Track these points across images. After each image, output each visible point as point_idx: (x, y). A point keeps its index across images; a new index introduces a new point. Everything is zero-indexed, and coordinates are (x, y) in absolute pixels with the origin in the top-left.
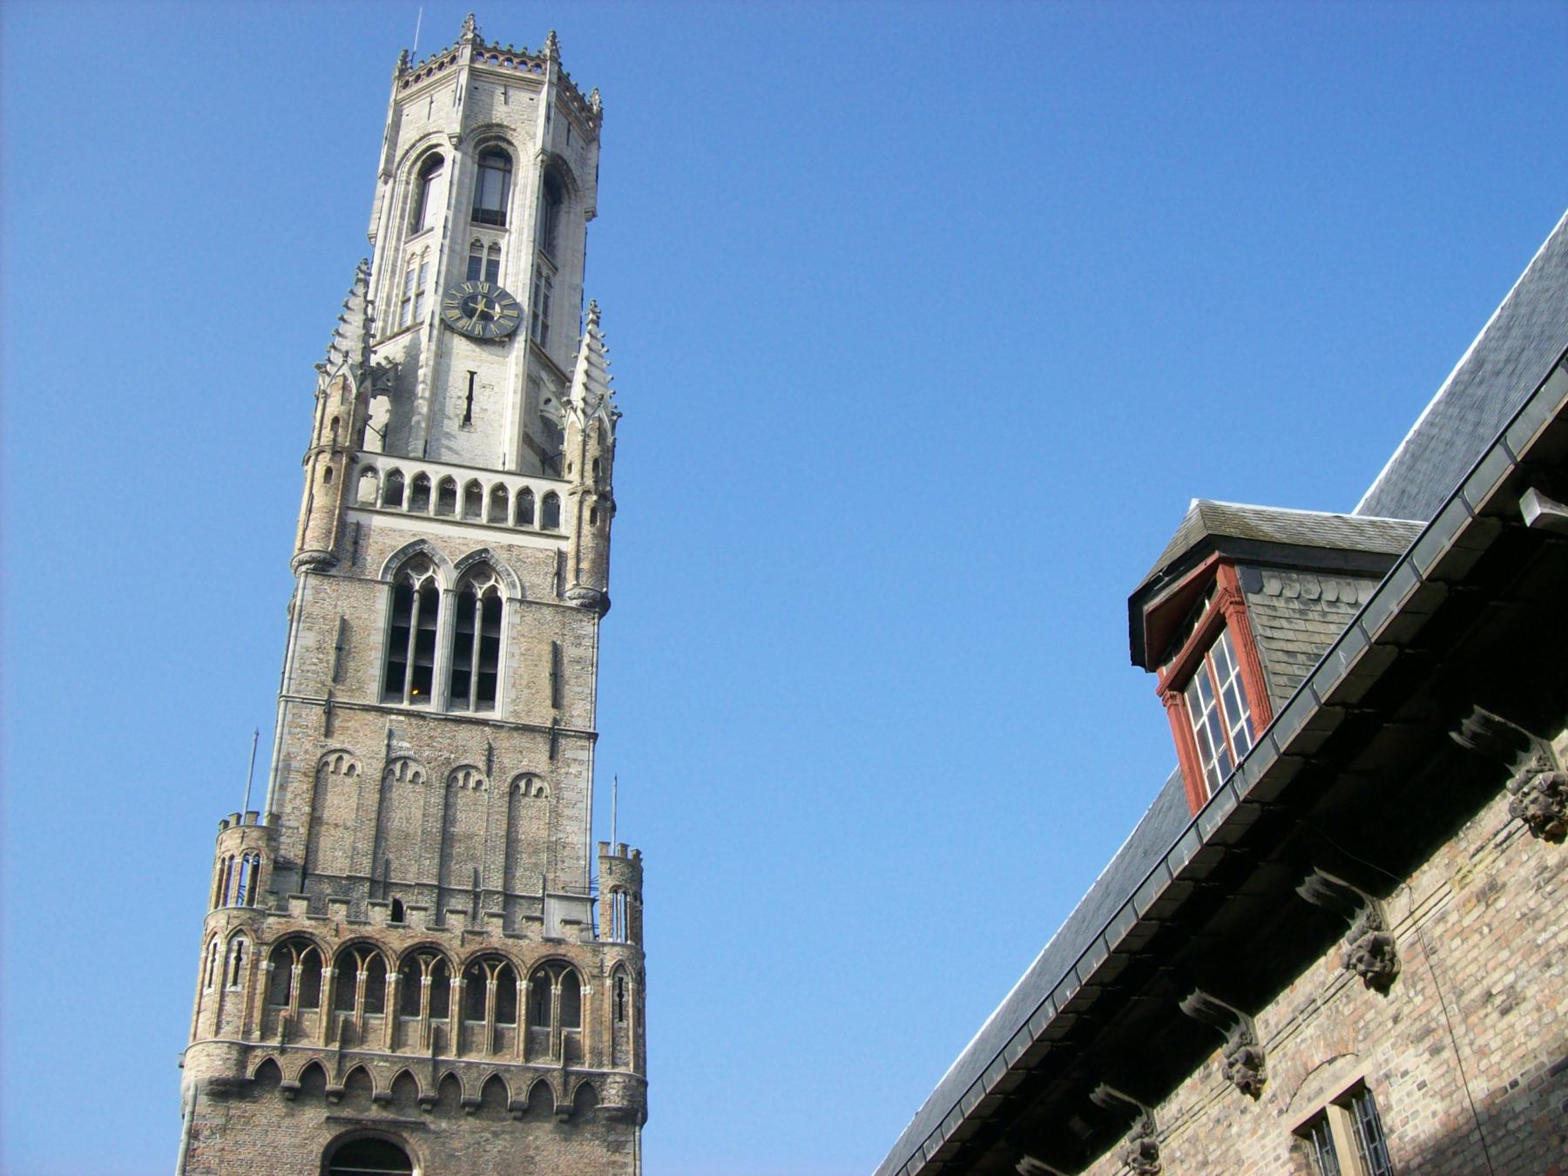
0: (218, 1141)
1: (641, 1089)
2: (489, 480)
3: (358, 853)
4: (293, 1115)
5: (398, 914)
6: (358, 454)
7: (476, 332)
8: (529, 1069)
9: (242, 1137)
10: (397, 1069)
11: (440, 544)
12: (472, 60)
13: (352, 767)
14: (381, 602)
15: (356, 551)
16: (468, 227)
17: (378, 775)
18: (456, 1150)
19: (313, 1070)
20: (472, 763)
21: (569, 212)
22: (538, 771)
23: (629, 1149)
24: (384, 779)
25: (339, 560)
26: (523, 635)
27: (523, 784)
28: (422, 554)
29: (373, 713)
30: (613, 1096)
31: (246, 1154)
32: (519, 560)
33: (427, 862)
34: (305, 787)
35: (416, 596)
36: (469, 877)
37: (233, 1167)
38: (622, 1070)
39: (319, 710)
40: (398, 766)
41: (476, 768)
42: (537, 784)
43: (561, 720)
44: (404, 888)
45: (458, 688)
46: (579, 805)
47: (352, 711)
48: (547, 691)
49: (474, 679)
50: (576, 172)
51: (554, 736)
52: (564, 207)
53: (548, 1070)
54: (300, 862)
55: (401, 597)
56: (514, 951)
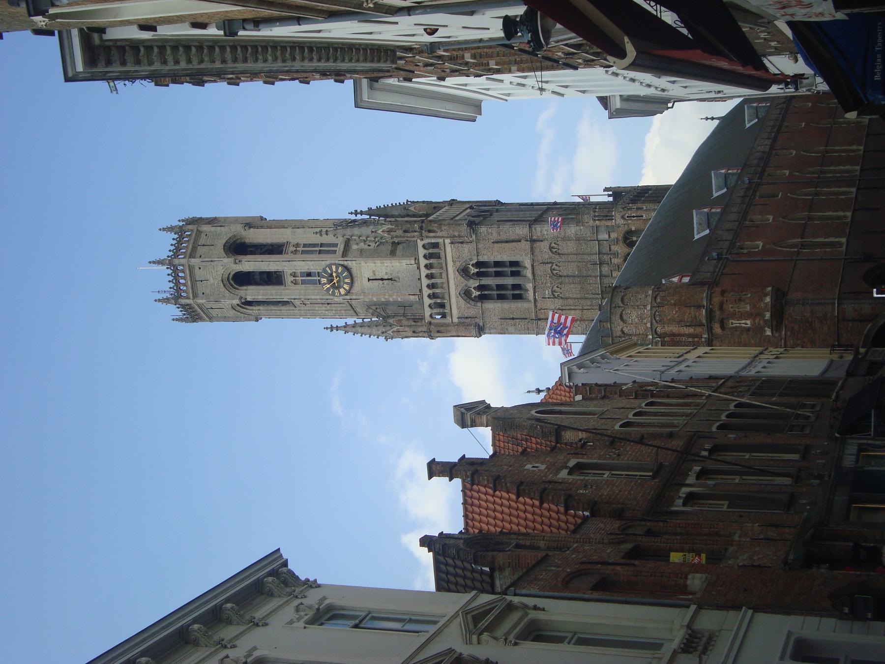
2: (424, 272)
6: (426, 321)
7: (349, 281)
11: (459, 289)
15: (470, 317)
16: (287, 287)
17: (561, 301)
20: (549, 269)
26: (492, 254)
39: (539, 322)
40: (556, 294)
41: (551, 267)
42: (553, 245)
48: (514, 243)
52: (247, 241)
55: (483, 298)
56: (623, 255)
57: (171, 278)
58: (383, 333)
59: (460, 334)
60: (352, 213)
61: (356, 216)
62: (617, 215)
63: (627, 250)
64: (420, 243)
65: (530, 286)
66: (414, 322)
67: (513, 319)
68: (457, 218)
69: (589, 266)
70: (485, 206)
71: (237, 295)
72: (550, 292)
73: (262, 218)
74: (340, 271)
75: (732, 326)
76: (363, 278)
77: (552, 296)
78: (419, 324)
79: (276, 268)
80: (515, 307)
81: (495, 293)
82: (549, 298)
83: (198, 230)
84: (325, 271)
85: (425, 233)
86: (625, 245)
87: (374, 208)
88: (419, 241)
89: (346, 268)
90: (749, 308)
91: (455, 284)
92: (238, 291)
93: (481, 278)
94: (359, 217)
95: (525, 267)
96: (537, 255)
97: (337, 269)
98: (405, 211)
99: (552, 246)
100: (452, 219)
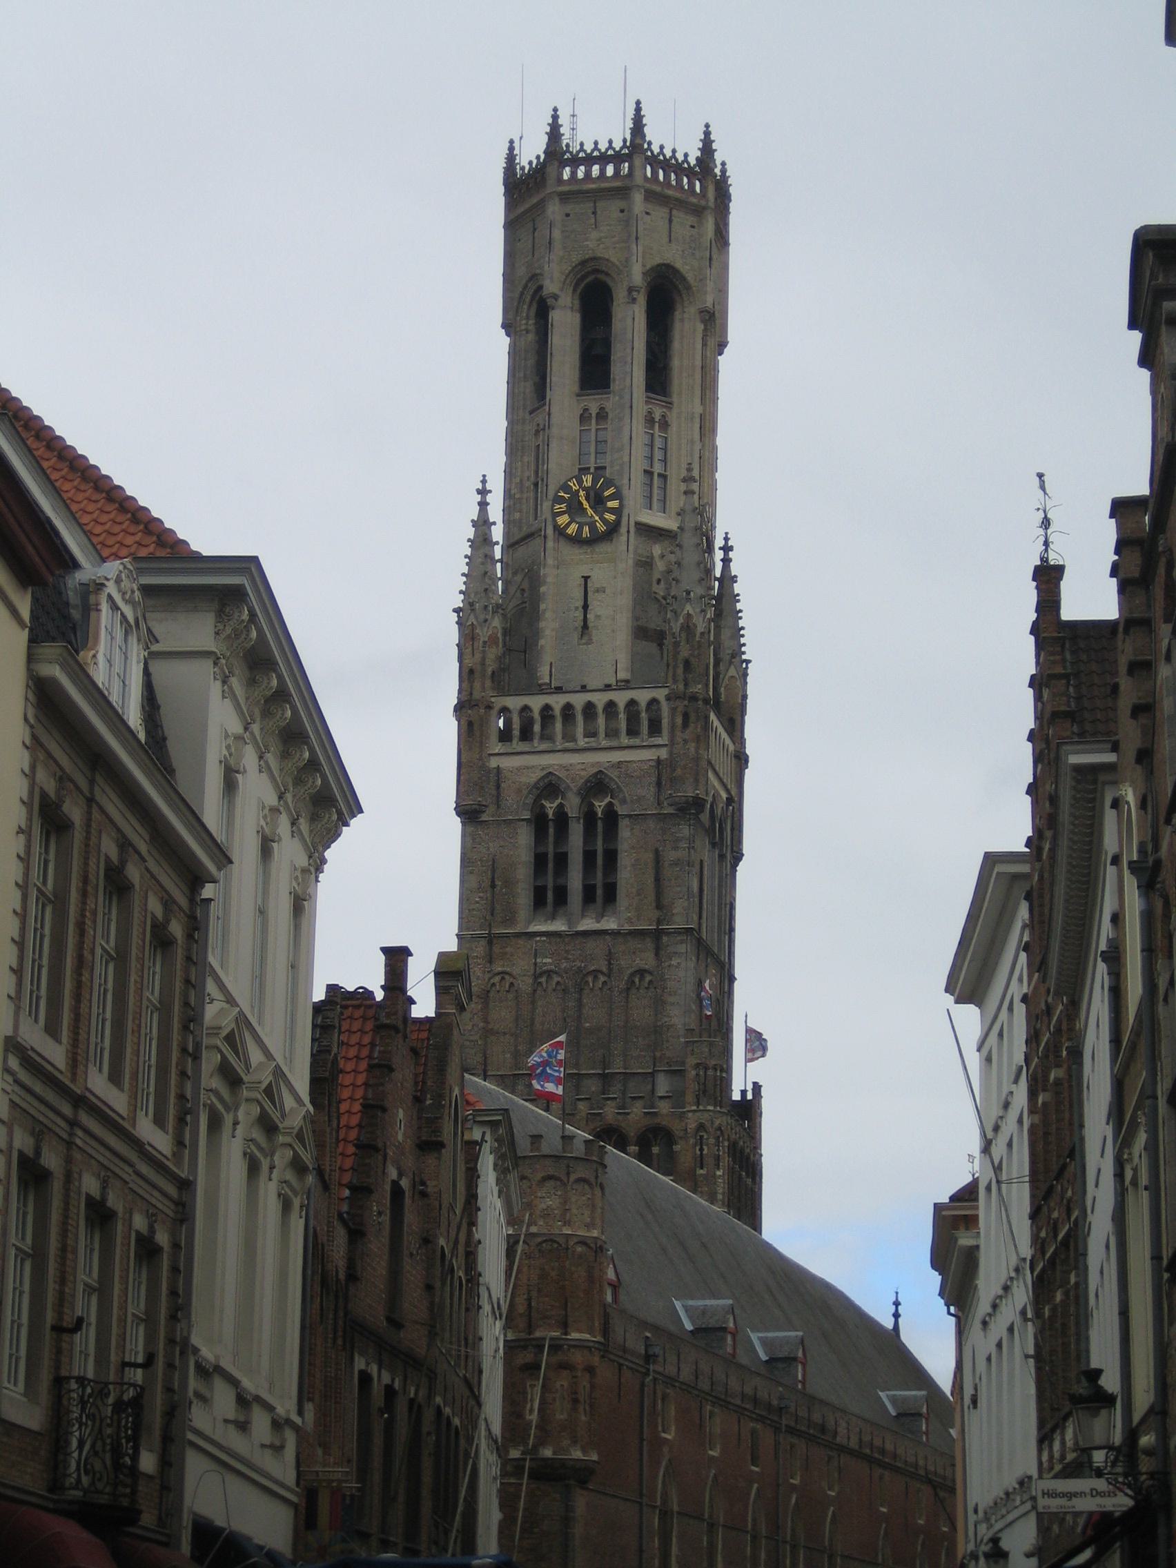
2: (599, 700)
6: (493, 699)
7: (584, 536)
11: (562, 774)
13: (512, 984)
21: (682, 320)
24: (535, 991)
26: (633, 848)
27: (637, 980)
28: (550, 784)
29: (523, 937)
34: (480, 1007)
35: (551, 824)
39: (483, 942)
40: (543, 980)
42: (648, 978)
46: (679, 991)
52: (678, 315)
55: (539, 822)
56: (623, 1125)
57: (603, 146)
58: (471, 604)
59: (463, 771)
60: (726, 539)
61: (720, 548)
62: (706, 1115)
64: (661, 694)
65: (559, 926)
66: (493, 673)
67: (493, 886)
68: (711, 775)
70: (732, 829)
71: (562, 290)
73: (722, 346)
74: (610, 517)
75: (528, 1384)
78: (488, 683)
79: (617, 378)
81: (551, 849)
82: (535, 964)
83: (704, 208)
84: (609, 483)
85: (681, 705)
87: (737, 588)
88: (666, 691)
89: (613, 530)
90: (562, 1417)
92: (572, 288)
93: (582, 821)
94: (719, 555)
95: (603, 916)
97: (612, 511)
98: (728, 657)
99: (646, 975)
100: (709, 763)
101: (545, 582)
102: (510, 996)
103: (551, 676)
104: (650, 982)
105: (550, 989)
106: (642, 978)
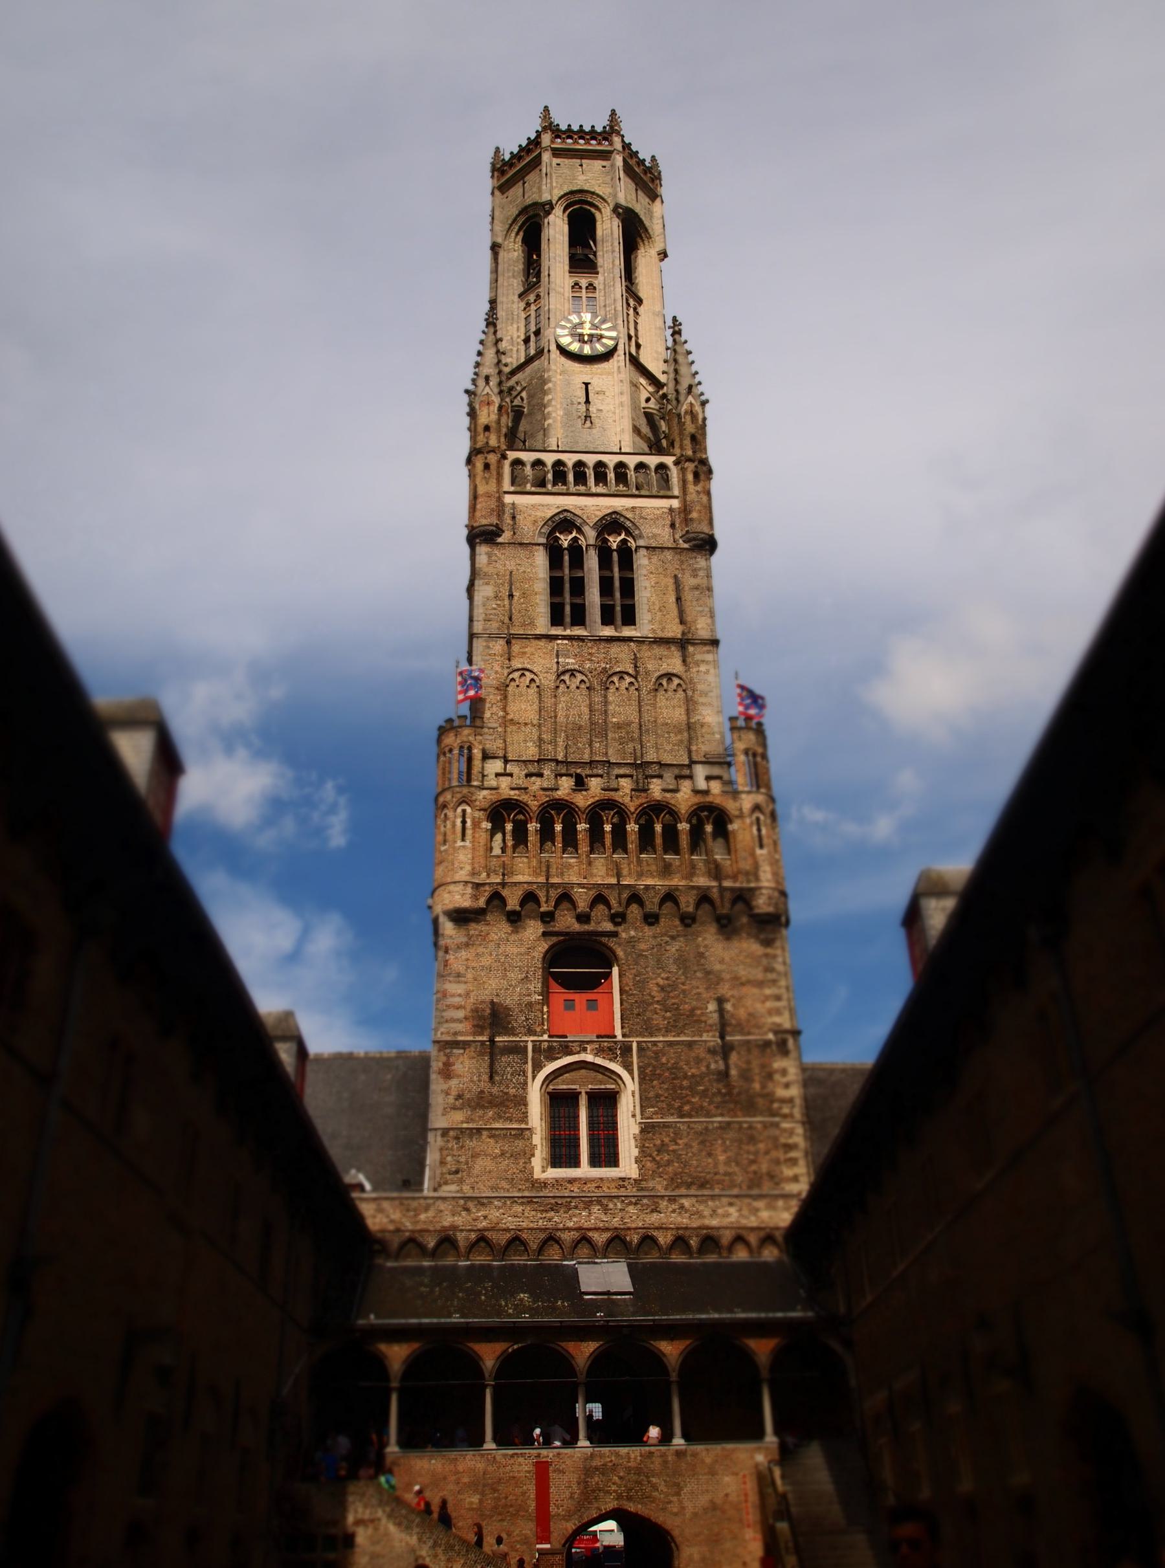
0: (463, 954)
1: (783, 899)
2: (611, 460)
3: (544, 742)
4: (517, 932)
5: (580, 783)
8: (693, 887)
9: (481, 950)
10: (593, 893)
12: (552, 142)
13: (532, 680)
14: (541, 559)
17: (552, 685)
18: (643, 951)
19: (530, 898)
20: (623, 670)
22: (675, 671)
23: (778, 943)
25: (503, 532)
26: (651, 573)
27: (664, 682)
28: (565, 520)
29: (543, 640)
30: (762, 904)
31: (486, 961)
32: (642, 518)
33: (598, 745)
34: (498, 698)
35: (566, 552)
36: (631, 754)
37: (477, 971)
38: (766, 884)
39: (502, 642)
40: (566, 677)
41: (628, 674)
42: (676, 681)
43: (689, 632)
44: (581, 765)
45: (607, 618)
47: (527, 640)
48: (674, 612)
49: (618, 608)
50: (647, 223)
51: (683, 644)
52: (641, 252)
53: (709, 888)
54: (501, 754)
55: (554, 553)
56: (672, 802)
59: (480, 500)
63: (683, 812)
64: (669, 460)
67: (511, 596)
69: (631, 745)
72: (573, 667)
76: (590, 376)
77: (561, 669)
80: (538, 601)
82: (558, 663)
85: (690, 466)
86: (695, 807)
88: (673, 459)
91: (586, 506)
92: (562, 208)
96: (653, 649)
97: (611, 338)
99: (674, 679)
101: (550, 381)
102: (533, 690)
103: (558, 446)
104: (679, 685)
105: (573, 686)
106: (670, 680)
